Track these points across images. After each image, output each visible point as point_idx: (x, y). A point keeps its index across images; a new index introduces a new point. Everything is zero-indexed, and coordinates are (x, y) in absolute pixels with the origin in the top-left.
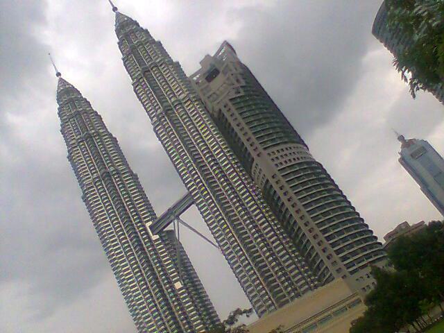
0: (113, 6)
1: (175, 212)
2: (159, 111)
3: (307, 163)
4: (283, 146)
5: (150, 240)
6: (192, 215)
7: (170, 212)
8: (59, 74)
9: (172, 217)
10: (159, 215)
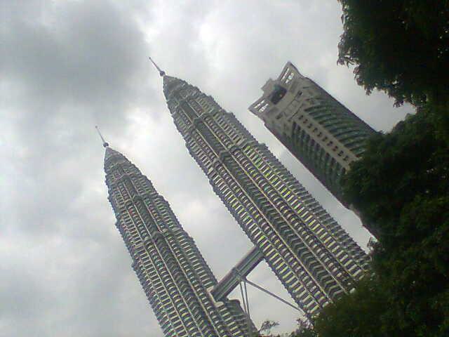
1: (241, 272)
2: (215, 161)
5: (213, 308)
6: (262, 272)
7: (235, 271)
8: (106, 145)
9: (238, 278)
10: (219, 279)
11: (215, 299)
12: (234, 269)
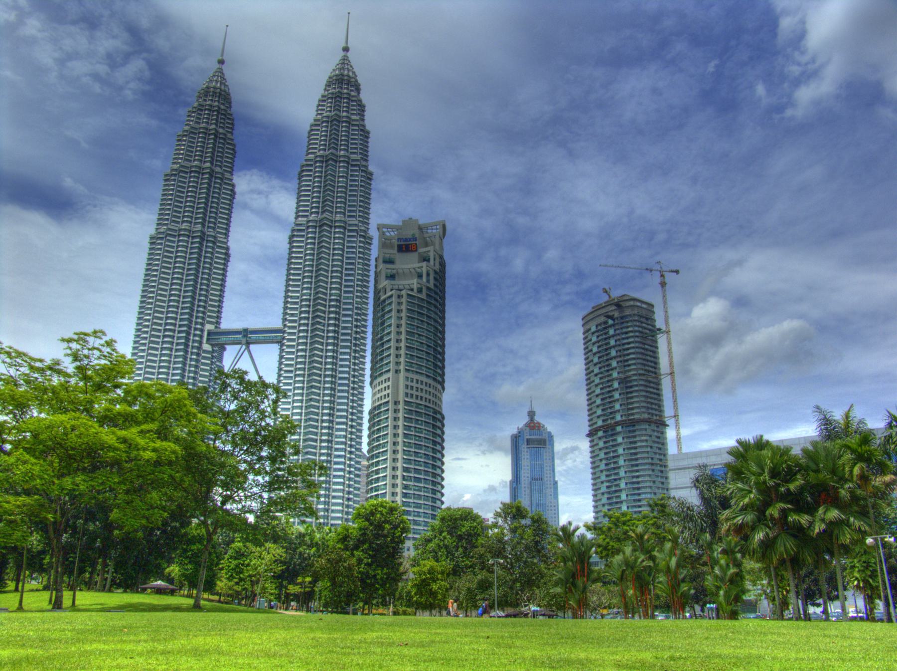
0: (347, 42)
3: (436, 412)
4: (425, 379)
5: (199, 348)
7: (245, 332)
10: (225, 325)
11: (208, 340)
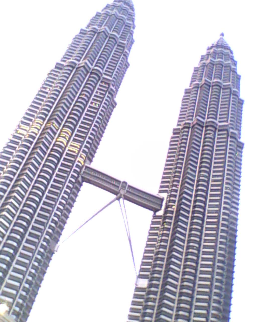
12: (125, 183)
